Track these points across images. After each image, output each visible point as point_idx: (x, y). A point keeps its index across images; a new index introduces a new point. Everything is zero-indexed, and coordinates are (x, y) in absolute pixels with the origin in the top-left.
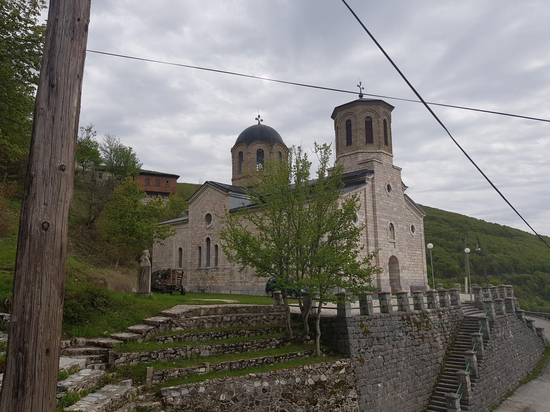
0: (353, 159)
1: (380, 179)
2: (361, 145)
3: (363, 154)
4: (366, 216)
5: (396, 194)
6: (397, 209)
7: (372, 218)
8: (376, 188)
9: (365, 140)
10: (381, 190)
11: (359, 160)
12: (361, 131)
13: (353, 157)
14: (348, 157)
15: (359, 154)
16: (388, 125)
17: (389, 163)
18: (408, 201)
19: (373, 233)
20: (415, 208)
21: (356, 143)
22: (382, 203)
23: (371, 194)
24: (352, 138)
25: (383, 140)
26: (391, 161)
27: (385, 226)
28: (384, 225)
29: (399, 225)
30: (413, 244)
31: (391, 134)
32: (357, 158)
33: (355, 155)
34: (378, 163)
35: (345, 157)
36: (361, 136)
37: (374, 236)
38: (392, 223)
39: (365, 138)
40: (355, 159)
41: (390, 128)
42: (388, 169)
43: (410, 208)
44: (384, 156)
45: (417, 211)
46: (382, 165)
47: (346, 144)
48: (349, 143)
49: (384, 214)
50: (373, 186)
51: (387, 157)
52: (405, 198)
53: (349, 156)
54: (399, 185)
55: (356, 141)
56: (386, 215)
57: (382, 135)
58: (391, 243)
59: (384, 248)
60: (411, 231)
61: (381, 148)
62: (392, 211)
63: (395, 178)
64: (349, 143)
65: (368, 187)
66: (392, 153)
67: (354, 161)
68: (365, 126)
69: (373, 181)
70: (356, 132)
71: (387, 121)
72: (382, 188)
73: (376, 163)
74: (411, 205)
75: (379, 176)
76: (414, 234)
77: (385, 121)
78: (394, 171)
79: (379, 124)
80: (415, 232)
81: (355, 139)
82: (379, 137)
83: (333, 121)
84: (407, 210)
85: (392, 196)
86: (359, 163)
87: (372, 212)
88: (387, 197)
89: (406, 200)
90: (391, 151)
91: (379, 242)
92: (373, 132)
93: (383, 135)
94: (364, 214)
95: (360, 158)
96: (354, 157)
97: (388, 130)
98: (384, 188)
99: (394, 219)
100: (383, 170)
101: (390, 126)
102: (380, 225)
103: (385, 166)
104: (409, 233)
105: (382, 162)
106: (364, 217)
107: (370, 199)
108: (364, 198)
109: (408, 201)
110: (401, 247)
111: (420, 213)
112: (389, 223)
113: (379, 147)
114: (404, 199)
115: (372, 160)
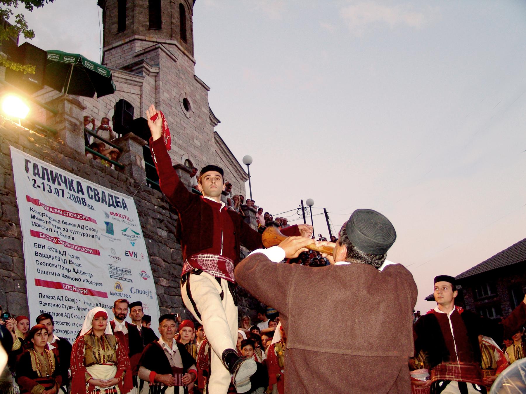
0: (126, 51)
1: (170, 81)
2: (141, 29)
3: (144, 42)
5: (200, 121)
6: (201, 143)
8: (161, 91)
9: (148, 23)
10: (172, 100)
11: (136, 51)
12: (141, 9)
13: (126, 47)
14: (119, 50)
15: (136, 41)
16: (188, 16)
17: (188, 68)
18: (220, 145)
20: (233, 160)
21: (132, 26)
22: (172, 120)
23: (152, 99)
24: (127, 19)
25: (178, 30)
26: (193, 69)
28: (175, 157)
31: (192, 30)
32: (133, 49)
33: (129, 44)
34: (168, 57)
35: (113, 50)
36: (141, 16)
38: (191, 160)
39: (147, 20)
40: (129, 50)
41: (191, 22)
42: (186, 75)
43: (223, 158)
44: (178, 53)
45: (235, 166)
46: (174, 63)
47: (116, 30)
48: (122, 27)
50: (157, 88)
51: (183, 57)
52: (215, 138)
53: (120, 47)
54: (206, 110)
55: (133, 23)
56: (180, 142)
57: (176, 20)
61: (173, 38)
62: (191, 142)
63: (198, 96)
64: (122, 27)
65: (148, 82)
66: (193, 55)
67: (129, 54)
68: (148, 3)
69: (157, 80)
70: (133, 11)
71: (186, 9)
72: (174, 97)
73: (164, 54)
74: (225, 152)
75: (169, 77)
77: (181, 6)
78: (196, 85)
79: (172, 4)
81: (132, 21)
82: (172, 23)
83: (101, 10)
84: (218, 159)
85: (192, 119)
86: (135, 54)
88: (183, 116)
89: (218, 142)
90: (192, 52)
92: (162, 14)
93: (179, 23)
95: (138, 47)
96: (129, 47)
97: (188, 23)
98: (178, 100)
99: (194, 156)
100: (177, 72)
101: (191, 19)
103: (179, 67)
105: (174, 58)
108: (139, 100)
109: (220, 145)
111: (239, 172)
112: (185, 158)
113: (171, 37)
114: (213, 140)
115: (157, 46)
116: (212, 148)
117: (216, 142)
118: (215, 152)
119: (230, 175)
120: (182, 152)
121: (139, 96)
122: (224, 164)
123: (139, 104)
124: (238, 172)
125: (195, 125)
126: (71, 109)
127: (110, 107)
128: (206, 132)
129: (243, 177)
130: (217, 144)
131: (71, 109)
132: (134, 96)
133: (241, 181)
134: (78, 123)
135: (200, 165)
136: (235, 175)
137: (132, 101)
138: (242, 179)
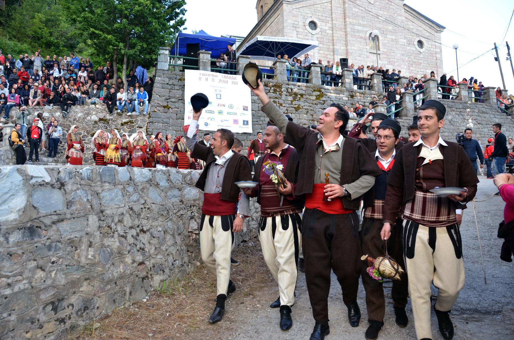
4: (332, 24)
7: (343, 27)
18: (410, 12)
19: (344, 42)
22: (357, 10)
27: (363, 35)
28: (360, 34)
29: (388, 36)
30: (422, 61)
37: (345, 46)
43: (415, 20)
45: (428, 24)
49: (361, 22)
56: (365, 23)
58: (371, 54)
59: (359, 58)
60: (417, 46)
76: (422, 50)
80: (423, 49)
84: (410, 23)
87: (343, 20)
88: (368, 4)
91: (349, 51)
94: (330, 22)
102: (353, 33)
104: (414, 49)
106: (330, 25)
107: (339, 5)
108: (330, 5)
110: (391, 59)
114: (403, 10)
116: (399, 17)
117: (406, 11)
118: (404, 18)
119: (423, 32)
120: (366, 29)
121: (330, 3)
122: (416, 25)
123: (330, 8)
124: (432, 27)
125: (379, 7)
126: (204, 56)
127: (307, 17)
128: (391, 9)
129: (437, 30)
130: (408, 12)
131: (204, 56)
132: (326, 4)
133: (436, 34)
134: (207, 61)
135: (384, 33)
136: (429, 30)
137: (325, 8)
138: (437, 32)
